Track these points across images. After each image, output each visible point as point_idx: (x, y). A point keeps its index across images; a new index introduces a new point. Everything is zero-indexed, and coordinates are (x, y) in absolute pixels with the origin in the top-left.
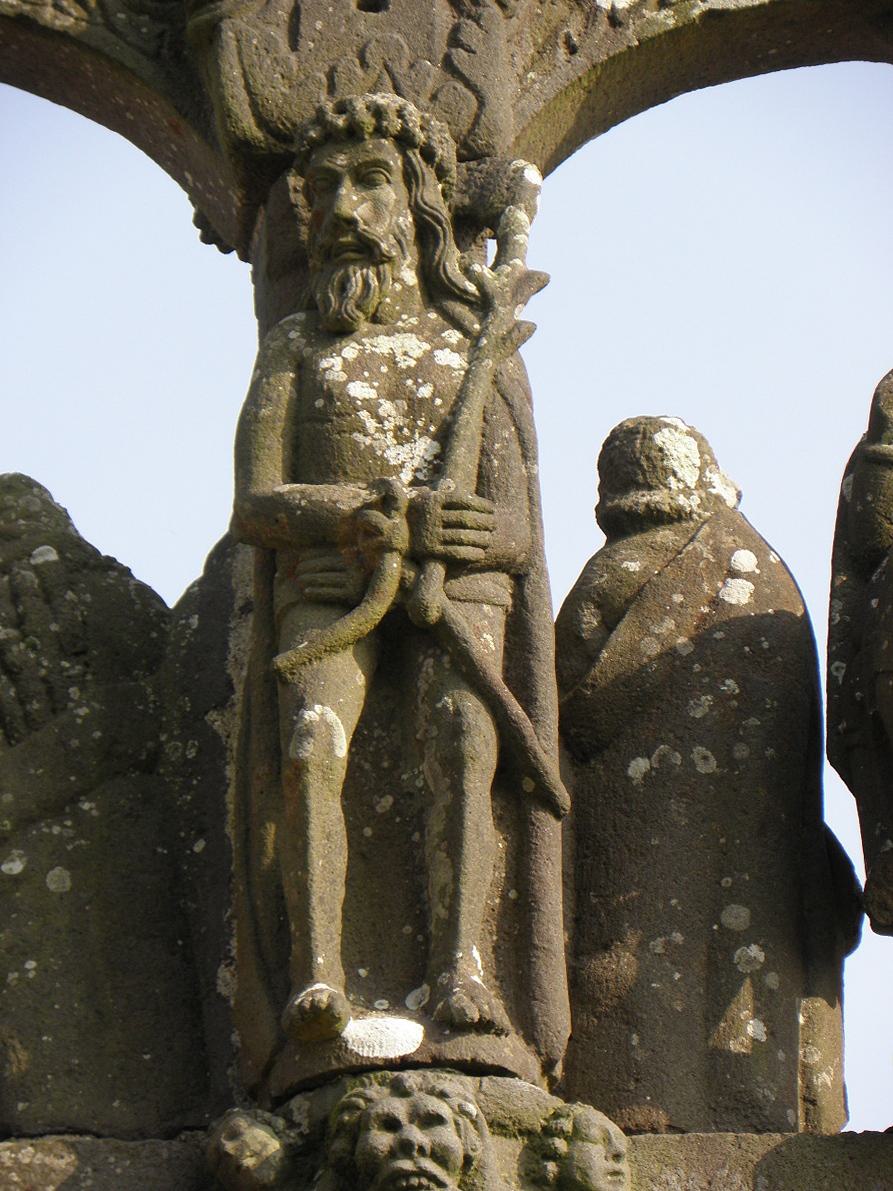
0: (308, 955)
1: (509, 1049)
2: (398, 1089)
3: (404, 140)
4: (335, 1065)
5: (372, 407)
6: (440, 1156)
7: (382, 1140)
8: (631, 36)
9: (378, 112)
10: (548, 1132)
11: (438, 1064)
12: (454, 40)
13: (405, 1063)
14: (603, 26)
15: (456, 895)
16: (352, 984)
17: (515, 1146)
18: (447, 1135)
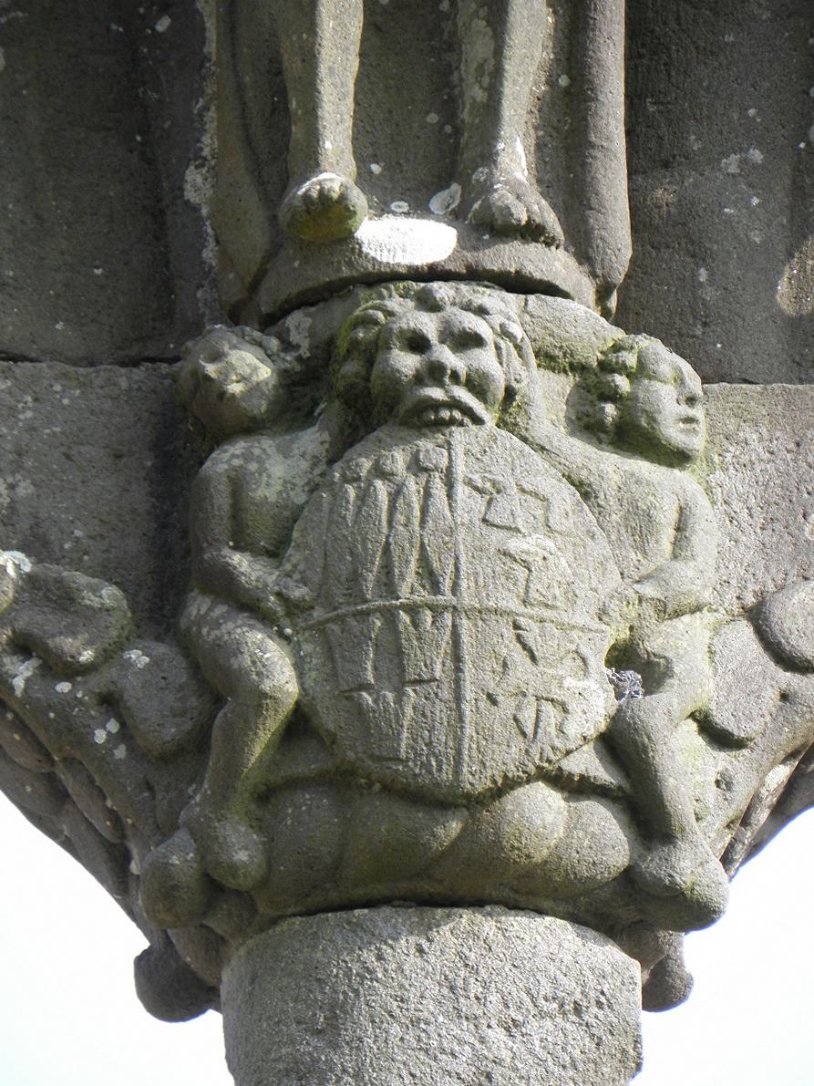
0: (313, 138)
1: (555, 263)
2: (428, 303)
4: (346, 272)
6: (478, 385)
7: (407, 363)
10: (606, 367)
11: (475, 275)
13: (435, 273)
15: (498, 73)
16: (364, 179)
17: (564, 384)
18: (485, 359)
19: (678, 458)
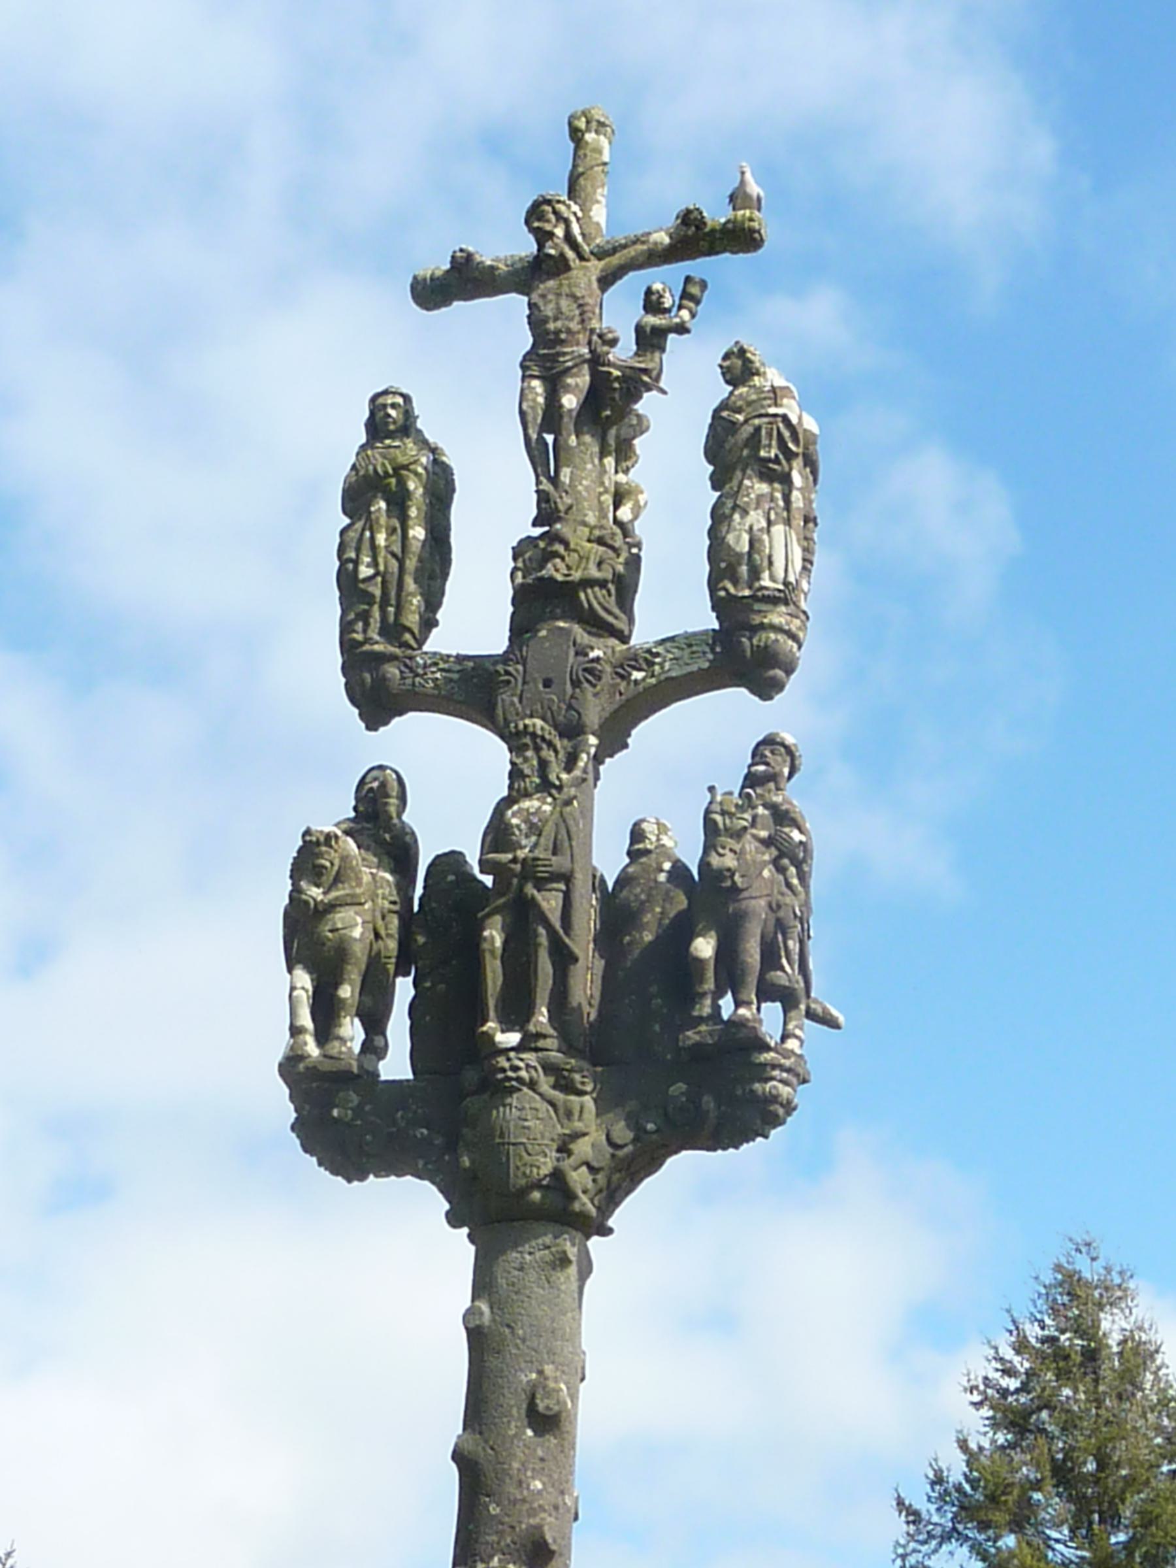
0: (488, 1015)
3: (534, 735)
5: (518, 826)
6: (519, 1080)
8: (641, 687)
9: (526, 726)
12: (572, 697)
14: (632, 684)
19: (581, 1093)
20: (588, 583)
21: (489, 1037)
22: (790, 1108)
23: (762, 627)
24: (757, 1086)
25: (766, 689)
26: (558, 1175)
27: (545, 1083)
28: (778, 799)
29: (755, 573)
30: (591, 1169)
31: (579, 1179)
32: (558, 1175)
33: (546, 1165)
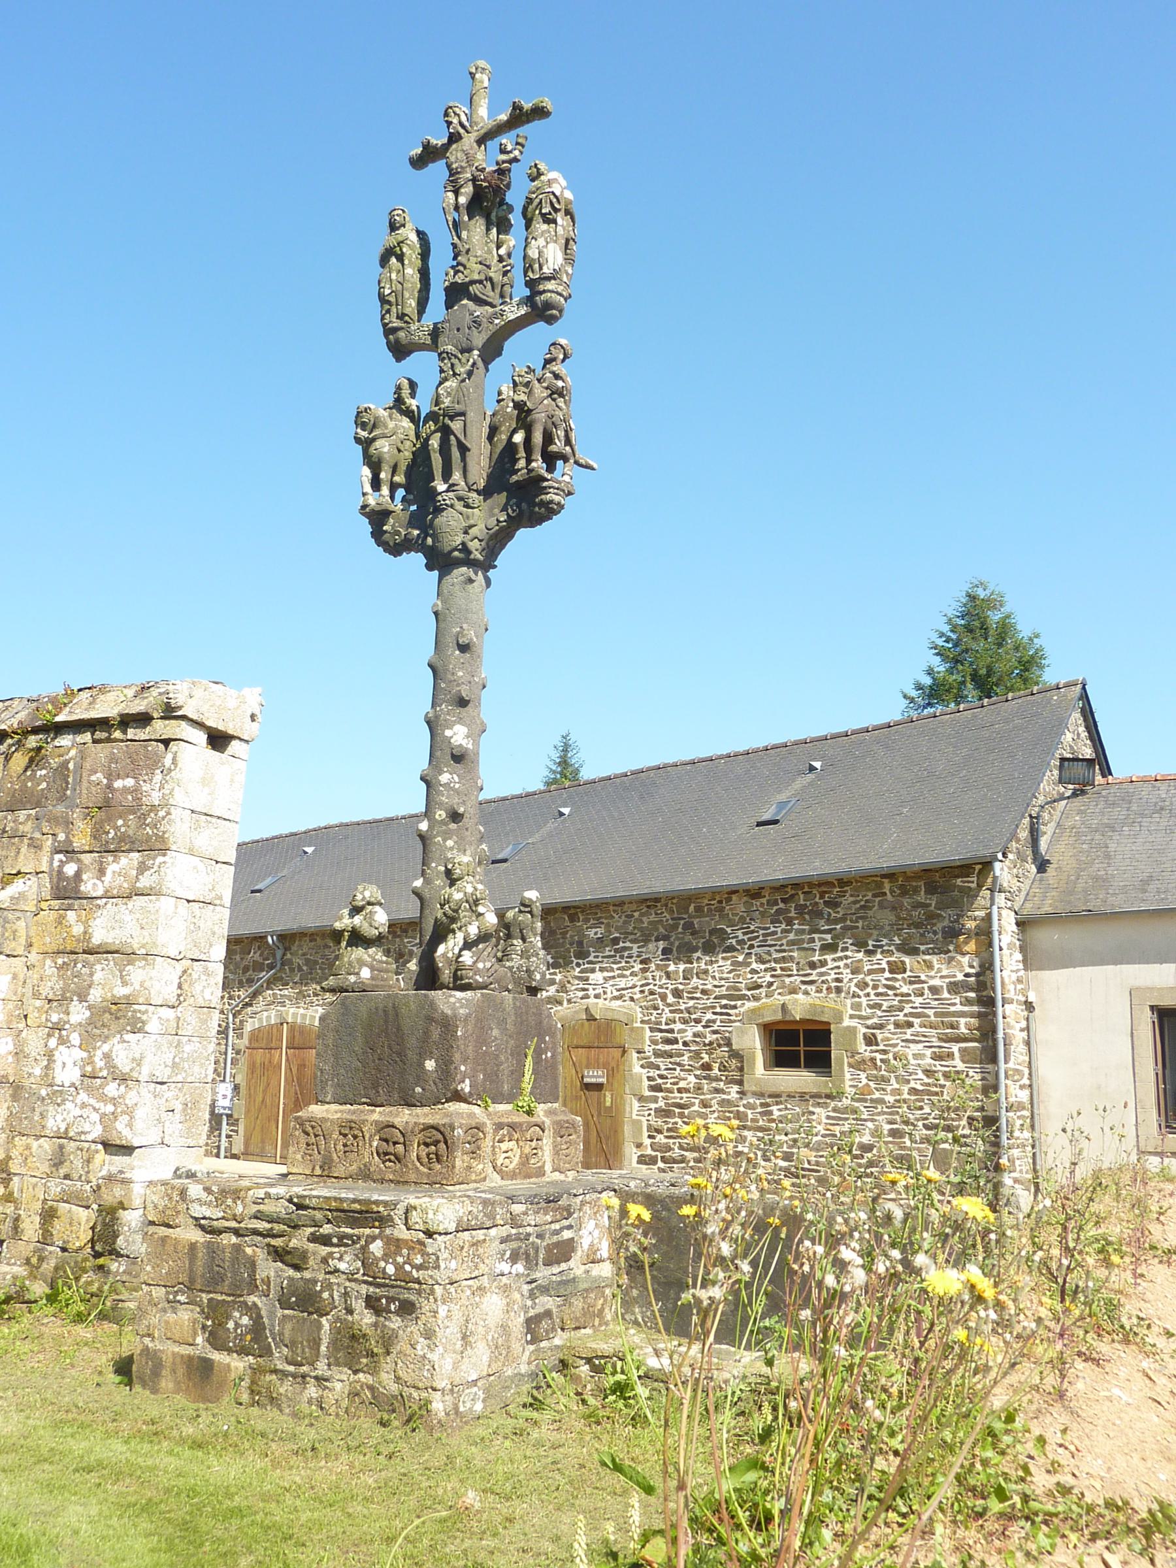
20: (473, 282)
21: (435, 488)
22: (561, 507)
23: (544, 291)
24: (543, 497)
25: (551, 320)
26: (463, 544)
27: (459, 505)
28: (555, 369)
29: (541, 268)
30: (480, 541)
31: (474, 545)
32: (463, 544)
33: (458, 540)
